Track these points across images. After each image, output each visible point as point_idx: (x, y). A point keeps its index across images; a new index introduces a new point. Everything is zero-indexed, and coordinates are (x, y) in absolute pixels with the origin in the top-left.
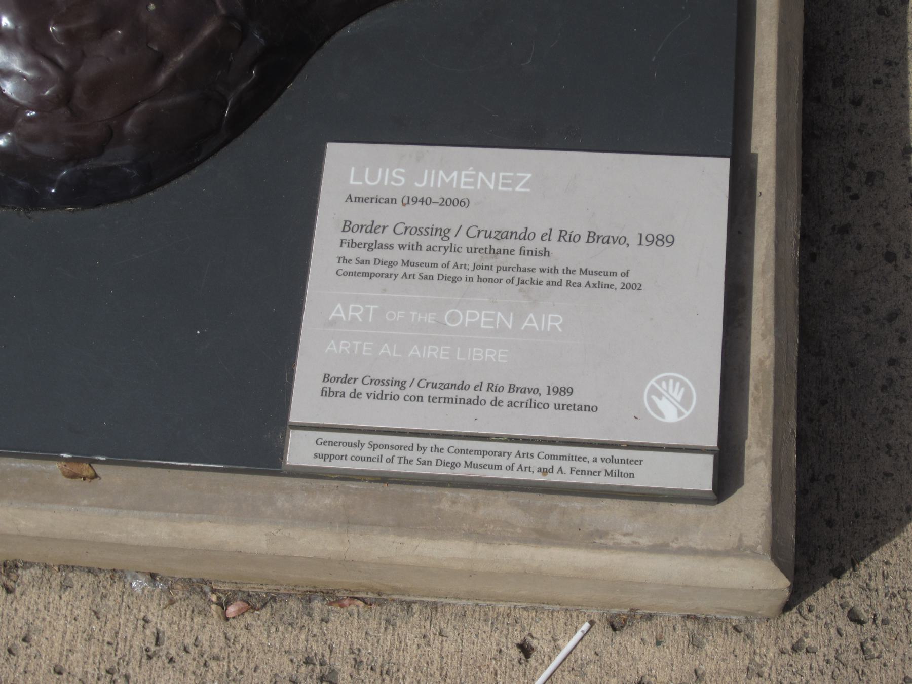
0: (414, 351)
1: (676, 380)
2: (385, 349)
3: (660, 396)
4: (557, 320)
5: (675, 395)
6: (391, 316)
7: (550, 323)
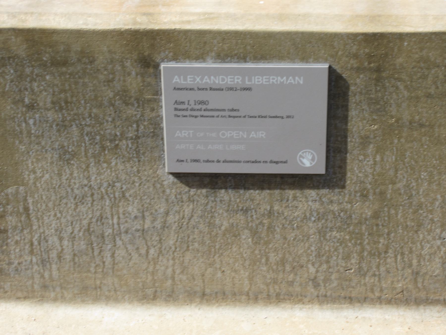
1: (309, 152)
3: (303, 158)
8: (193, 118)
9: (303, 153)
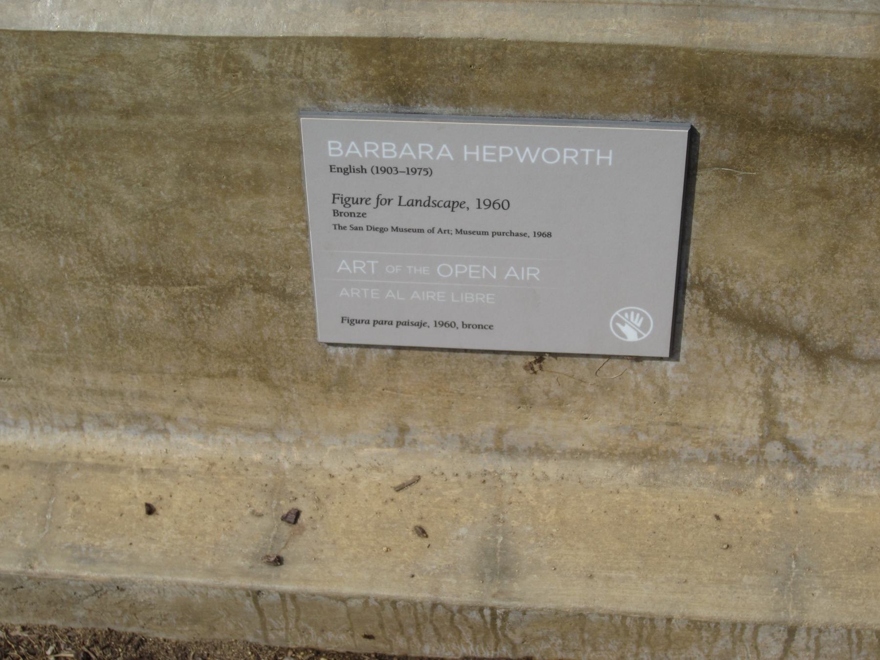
0: (415, 295)
1: (636, 312)
2: (390, 294)
3: (623, 323)
4: (535, 271)
5: (635, 322)
6: (390, 269)
7: (528, 274)
8: (377, 233)
9: (622, 313)
